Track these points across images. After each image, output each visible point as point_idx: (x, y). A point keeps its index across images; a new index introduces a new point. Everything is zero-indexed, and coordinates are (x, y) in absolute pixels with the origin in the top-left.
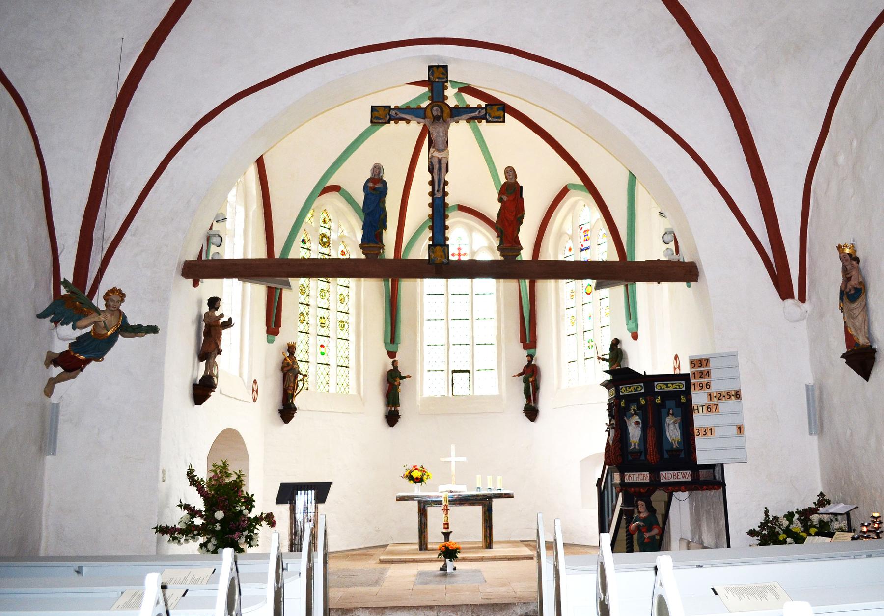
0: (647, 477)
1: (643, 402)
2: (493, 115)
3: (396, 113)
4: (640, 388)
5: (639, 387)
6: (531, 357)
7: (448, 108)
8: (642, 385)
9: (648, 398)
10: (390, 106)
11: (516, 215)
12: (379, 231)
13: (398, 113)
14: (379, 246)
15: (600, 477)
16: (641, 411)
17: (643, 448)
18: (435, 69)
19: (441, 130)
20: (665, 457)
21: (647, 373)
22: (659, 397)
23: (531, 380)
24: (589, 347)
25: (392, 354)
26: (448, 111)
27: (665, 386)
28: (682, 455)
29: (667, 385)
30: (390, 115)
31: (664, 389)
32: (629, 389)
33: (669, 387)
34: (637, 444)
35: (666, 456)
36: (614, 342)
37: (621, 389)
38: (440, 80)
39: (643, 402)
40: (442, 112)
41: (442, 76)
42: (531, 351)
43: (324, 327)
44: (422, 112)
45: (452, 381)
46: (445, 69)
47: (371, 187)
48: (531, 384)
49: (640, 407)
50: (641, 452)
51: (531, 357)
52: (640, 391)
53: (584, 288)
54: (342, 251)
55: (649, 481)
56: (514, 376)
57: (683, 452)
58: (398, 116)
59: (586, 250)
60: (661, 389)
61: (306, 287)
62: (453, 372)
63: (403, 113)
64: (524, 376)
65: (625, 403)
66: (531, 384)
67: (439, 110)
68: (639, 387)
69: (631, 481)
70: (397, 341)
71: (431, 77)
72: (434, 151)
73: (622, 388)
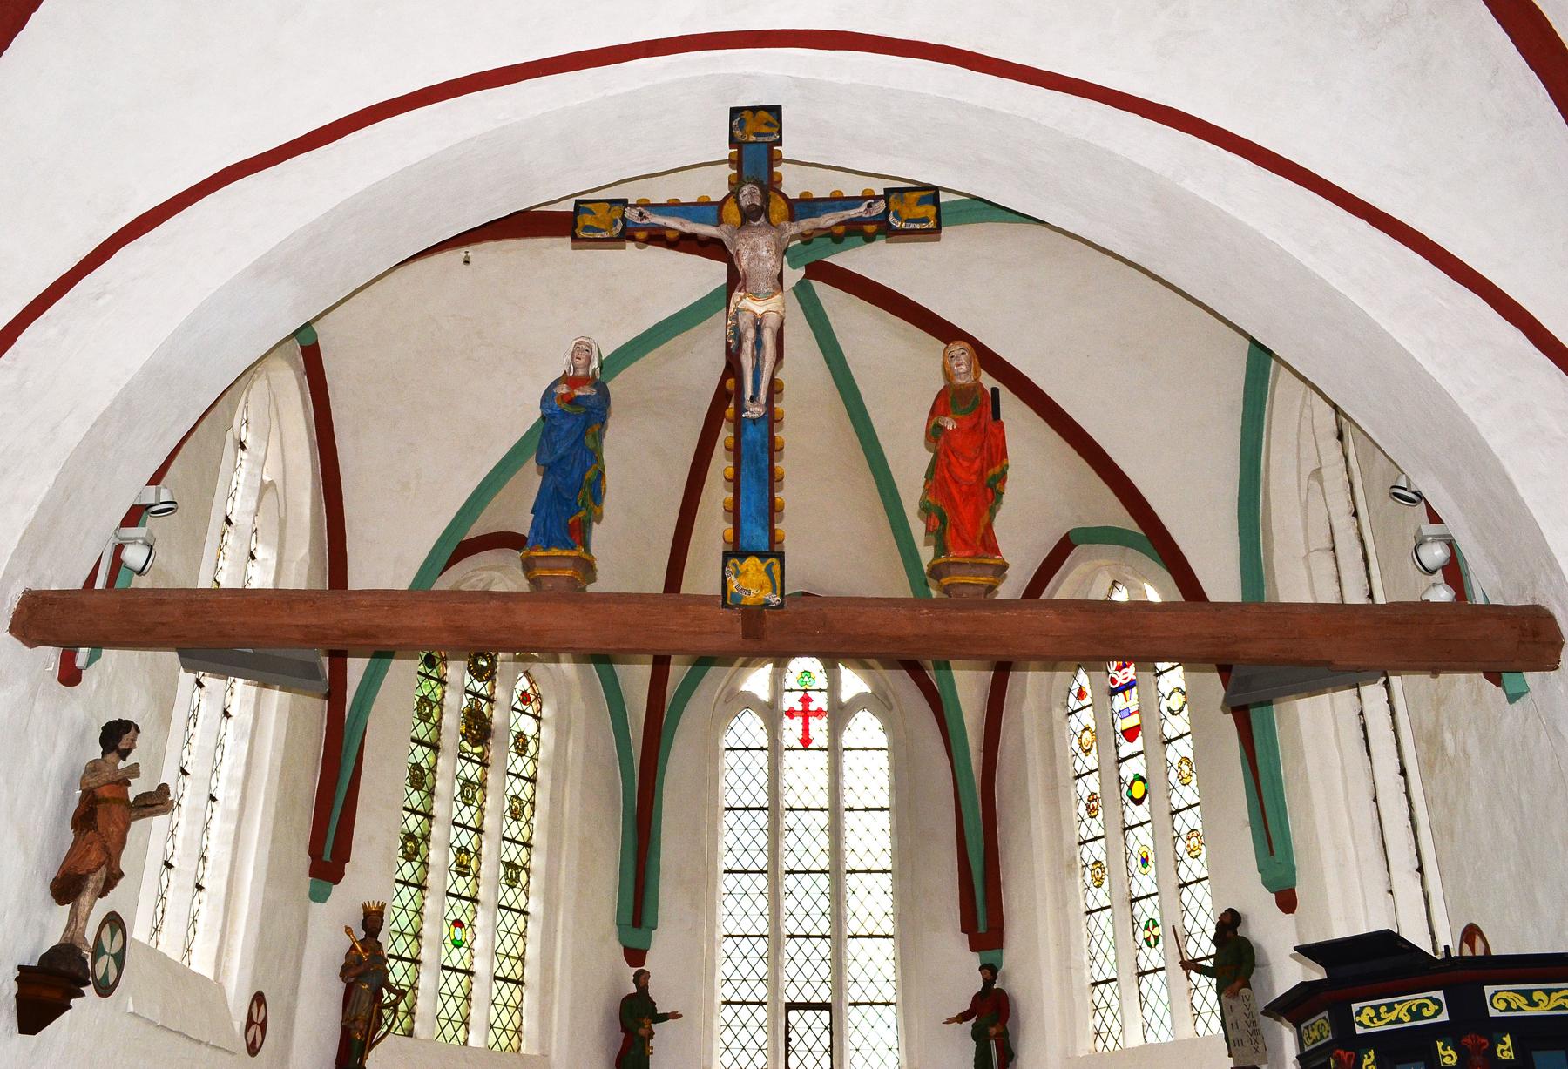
2: (906, 213)
3: (641, 214)
4: (1433, 1006)
6: (990, 971)
7: (782, 201)
8: (1439, 995)
9: (1467, 1040)
10: (627, 200)
11: (982, 471)
12: (581, 515)
13: (647, 213)
14: (574, 554)
18: (747, 115)
19: (761, 242)
22: (1507, 1039)
23: (993, 1031)
24: (1147, 940)
25: (635, 956)
26: (784, 207)
27: (1523, 1000)
29: (1527, 995)
30: (624, 219)
31: (1519, 1009)
32: (1388, 1012)
33: (1536, 1004)
36: (1228, 920)
37: (1359, 1013)
38: (761, 139)
40: (766, 199)
41: (765, 130)
42: (991, 956)
43: (468, 874)
44: (712, 212)
45: (787, 1033)
46: (775, 113)
47: (563, 396)
48: (993, 1043)
51: (990, 971)
52: (1434, 1016)
53: (1126, 788)
54: (524, 693)
56: (950, 1021)
58: (645, 222)
59: (1123, 691)
60: (1509, 1009)
61: (426, 772)
62: (792, 1006)
63: (660, 214)
64: (974, 1020)
66: (993, 1043)
67: (758, 193)
68: (1427, 1006)
70: (647, 919)
71: (738, 133)
72: (742, 298)
73: (1362, 1009)
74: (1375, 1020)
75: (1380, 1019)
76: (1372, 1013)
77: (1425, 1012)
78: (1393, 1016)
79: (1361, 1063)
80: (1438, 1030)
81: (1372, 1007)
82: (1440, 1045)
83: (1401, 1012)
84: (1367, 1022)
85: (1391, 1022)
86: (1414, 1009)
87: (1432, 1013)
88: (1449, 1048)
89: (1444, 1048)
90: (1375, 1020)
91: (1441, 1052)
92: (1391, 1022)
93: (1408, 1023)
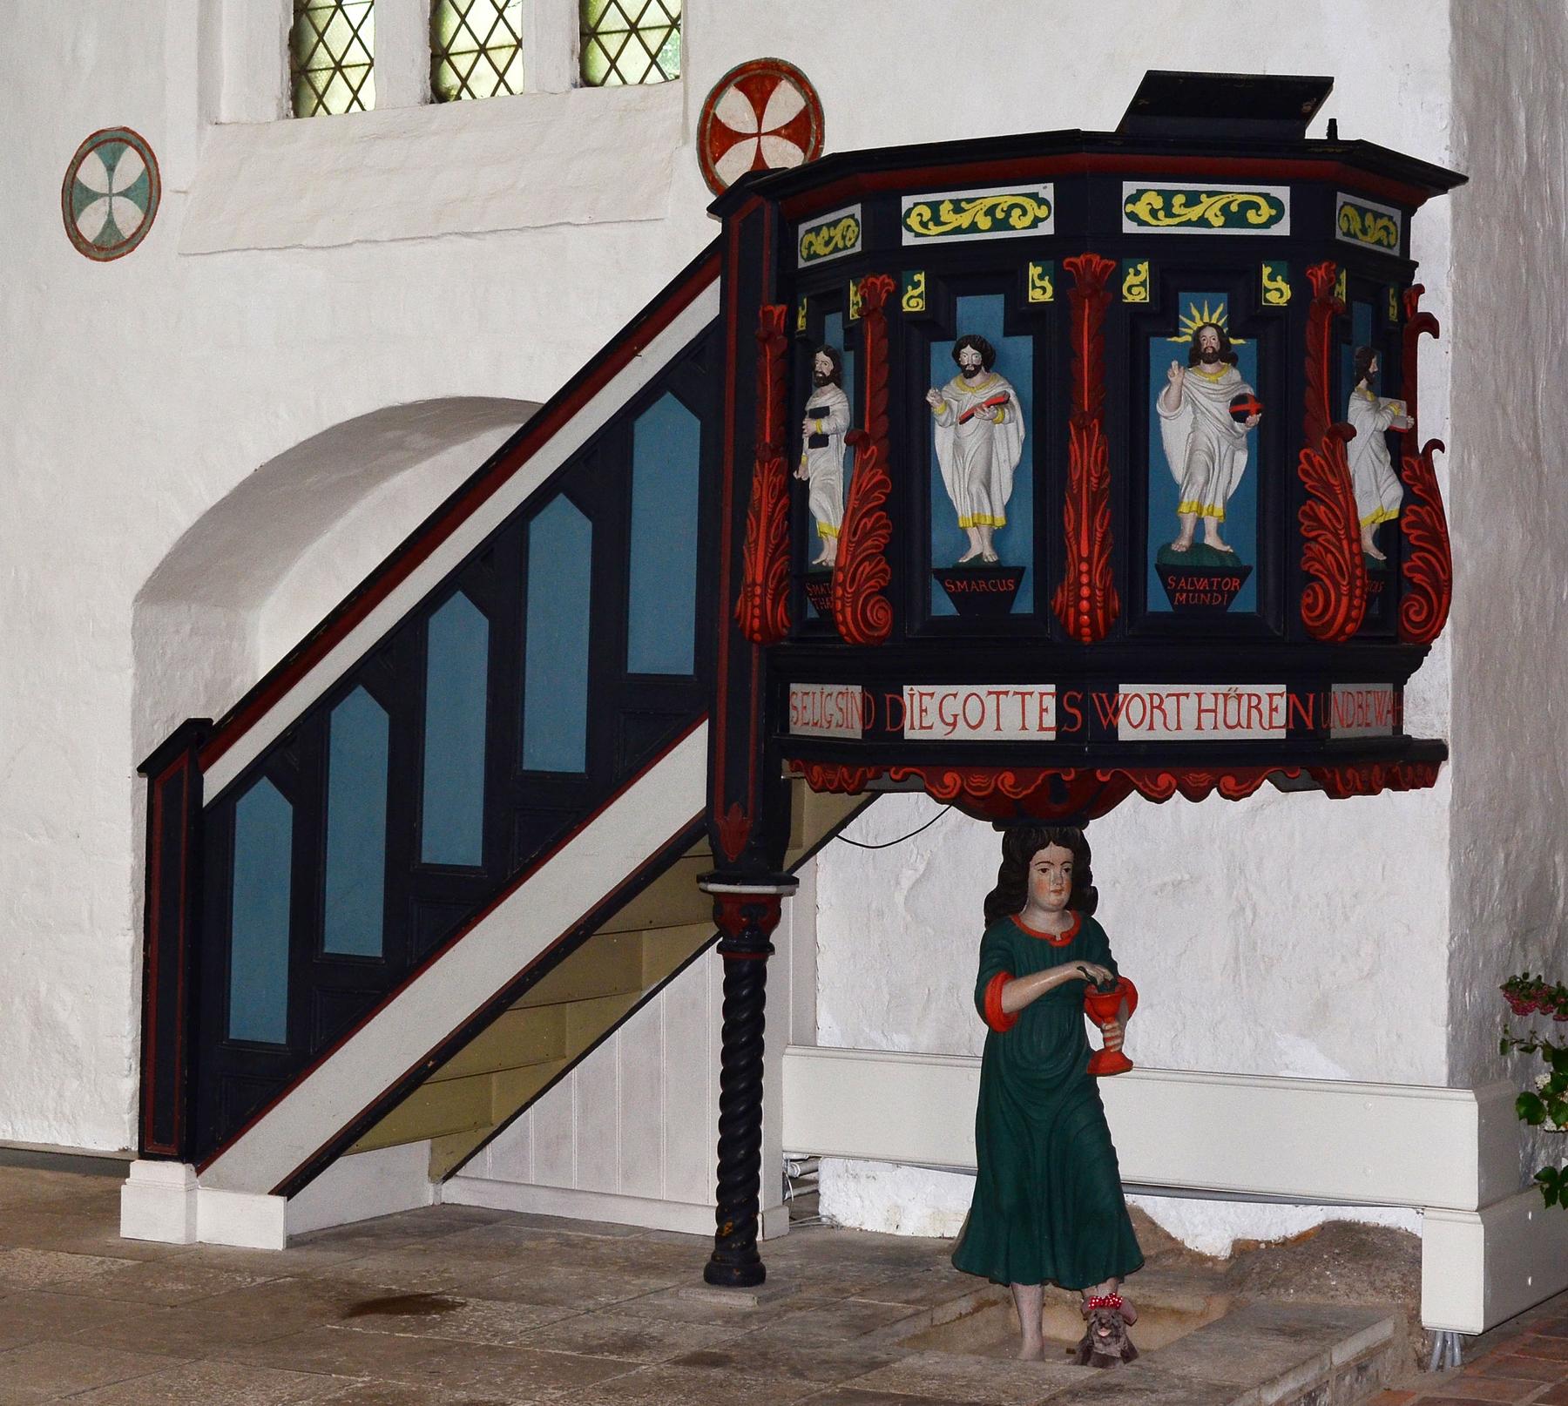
0: (1273, 710)
1: (1040, 291)
5: (1257, 207)
8: (1283, 193)
15: (216, 714)
16: (1253, 342)
17: (1022, 551)
20: (1152, 606)
21: (1342, 136)
28: (1024, 604)
32: (1187, 205)
34: (1211, 525)
35: (1158, 600)
37: (1134, 199)
39: (1277, 292)
49: (1021, 318)
50: (1242, 573)
52: (1266, 225)
57: (1252, 580)
65: (929, 296)
68: (1257, 207)
69: (1160, 734)
73: (1141, 193)
74: (1161, 214)
76: (1158, 203)
77: (1251, 216)
78: (1194, 213)
79: (1122, 281)
80: (1268, 248)
81: (1159, 192)
82: (1266, 271)
83: (1210, 209)
84: (1144, 214)
85: (1188, 223)
86: (1234, 208)
87: (1263, 219)
88: (1279, 278)
89: (1272, 278)
90: (1161, 214)
91: (1266, 282)
92: (1188, 223)
93: (1218, 228)
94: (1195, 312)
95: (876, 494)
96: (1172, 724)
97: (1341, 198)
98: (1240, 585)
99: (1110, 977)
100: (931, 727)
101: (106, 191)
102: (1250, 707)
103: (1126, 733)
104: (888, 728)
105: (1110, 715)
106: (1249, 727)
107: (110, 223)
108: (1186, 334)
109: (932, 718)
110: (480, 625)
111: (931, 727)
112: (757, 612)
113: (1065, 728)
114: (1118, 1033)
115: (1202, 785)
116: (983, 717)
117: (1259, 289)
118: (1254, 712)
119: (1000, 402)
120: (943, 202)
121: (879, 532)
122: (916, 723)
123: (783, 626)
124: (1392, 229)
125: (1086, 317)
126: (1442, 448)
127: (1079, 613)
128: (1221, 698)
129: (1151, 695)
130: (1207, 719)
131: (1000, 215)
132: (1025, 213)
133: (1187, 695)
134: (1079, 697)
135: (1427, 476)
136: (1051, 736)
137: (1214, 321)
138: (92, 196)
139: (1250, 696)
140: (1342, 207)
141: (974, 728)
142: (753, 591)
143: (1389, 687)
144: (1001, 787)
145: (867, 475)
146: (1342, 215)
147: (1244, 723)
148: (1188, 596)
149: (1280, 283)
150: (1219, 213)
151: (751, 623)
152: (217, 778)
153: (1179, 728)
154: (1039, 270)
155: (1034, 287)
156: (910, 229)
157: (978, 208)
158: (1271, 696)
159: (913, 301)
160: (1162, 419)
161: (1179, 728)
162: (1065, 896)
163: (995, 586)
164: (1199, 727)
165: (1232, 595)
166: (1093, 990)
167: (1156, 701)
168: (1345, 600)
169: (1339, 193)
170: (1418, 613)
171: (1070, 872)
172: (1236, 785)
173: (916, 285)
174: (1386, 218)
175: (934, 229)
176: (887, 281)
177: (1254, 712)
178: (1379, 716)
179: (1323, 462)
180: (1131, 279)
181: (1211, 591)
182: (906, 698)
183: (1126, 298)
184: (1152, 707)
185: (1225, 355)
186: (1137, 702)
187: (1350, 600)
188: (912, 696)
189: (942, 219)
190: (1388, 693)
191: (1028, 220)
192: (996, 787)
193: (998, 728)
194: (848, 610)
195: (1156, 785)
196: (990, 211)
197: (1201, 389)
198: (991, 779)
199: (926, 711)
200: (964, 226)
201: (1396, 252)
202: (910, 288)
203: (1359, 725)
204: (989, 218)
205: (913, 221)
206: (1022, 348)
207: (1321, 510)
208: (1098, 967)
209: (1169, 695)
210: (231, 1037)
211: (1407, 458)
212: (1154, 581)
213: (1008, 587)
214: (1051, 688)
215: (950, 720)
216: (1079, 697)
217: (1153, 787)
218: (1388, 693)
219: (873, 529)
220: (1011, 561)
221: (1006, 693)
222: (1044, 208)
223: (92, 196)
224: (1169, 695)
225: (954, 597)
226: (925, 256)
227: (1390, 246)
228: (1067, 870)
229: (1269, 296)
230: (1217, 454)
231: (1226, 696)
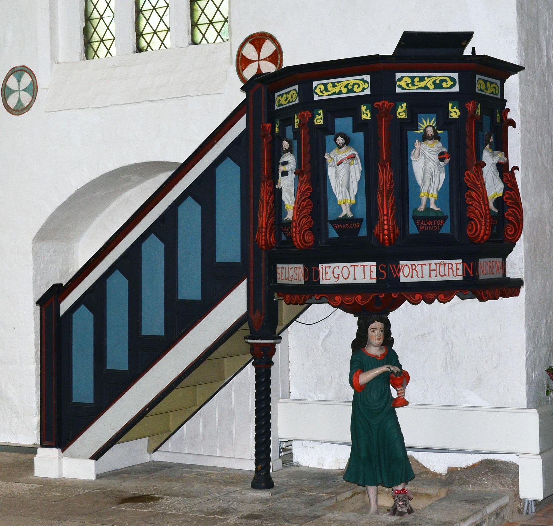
0: (457, 269)
1: (366, 115)
5: (446, 81)
8: (456, 76)
15: (64, 282)
17: (362, 213)
21: (478, 53)
28: (363, 232)
32: (420, 81)
34: (432, 200)
35: (413, 229)
37: (400, 79)
39: (455, 113)
49: (359, 125)
50: (444, 218)
55: (461, 278)
57: (448, 221)
65: (325, 118)
68: (446, 81)
69: (415, 279)
73: (402, 78)
74: (410, 85)
75: (413, 85)
76: (409, 81)
77: (444, 85)
78: (423, 84)
81: (410, 77)
83: (429, 82)
84: (404, 85)
85: (421, 88)
86: (438, 82)
88: (455, 107)
89: (452, 108)
90: (410, 85)
91: (450, 109)
92: (421, 88)
94: (424, 122)
95: (307, 193)
96: (420, 275)
97: (478, 77)
98: (444, 223)
99: (399, 370)
100: (329, 279)
101: (17, 89)
102: (449, 268)
103: (403, 279)
104: (314, 280)
105: (397, 273)
106: (449, 275)
107: (19, 101)
108: (421, 129)
109: (330, 276)
110: (161, 246)
111: (329, 279)
112: (264, 238)
113: (380, 278)
114: (403, 391)
115: (432, 298)
116: (349, 275)
117: (447, 112)
118: (450, 270)
119: (352, 157)
120: (328, 83)
121: (308, 207)
122: (324, 278)
123: (274, 243)
124: (497, 87)
125: (383, 124)
126: (518, 169)
127: (384, 235)
128: (438, 265)
129: (412, 265)
130: (433, 273)
131: (350, 87)
132: (359, 86)
133: (425, 264)
134: (385, 266)
135: (512, 180)
136: (375, 281)
137: (431, 124)
138: (13, 91)
139: (449, 264)
140: (478, 80)
141: (346, 279)
142: (262, 230)
143: (500, 259)
144: (356, 300)
145: (303, 186)
146: (478, 84)
147: (447, 274)
148: (424, 227)
149: (456, 109)
150: (432, 84)
151: (262, 242)
152: (65, 305)
153: (422, 277)
154: (365, 107)
155: (364, 114)
156: (316, 94)
157: (342, 85)
158: (457, 264)
159: (319, 120)
160: (413, 162)
161: (422, 277)
162: (381, 341)
163: (352, 226)
164: (430, 276)
165: (441, 226)
166: (393, 375)
167: (414, 267)
168: (483, 227)
169: (476, 75)
170: (511, 231)
171: (383, 332)
172: (444, 297)
173: (319, 115)
174: (494, 84)
175: (325, 93)
176: (308, 113)
177: (450, 270)
178: (497, 271)
179: (474, 176)
180: (400, 110)
181: (433, 225)
182: (320, 269)
183: (398, 117)
184: (412, 269)
185: (436, 137)
186: (406, 267)
187: (485, 228)
188: (322, 268)
189: (329, 90)
190: (500, 262)
191: (360, 89)
192: (355, 301)
193: (355, 279)
194: (298, 237)
195: (415, 299)
196: (346, 86)
197: (428, 150)
198: (353, 298)
199: (328, 273)
200: (336, 92)
201: (499, 96)
202: (317, 116)
203: (490, 274)
204: (346, 89)
205: (318, 91)
206: (360, 137)
207: (473, 194)
208: (395, 367)
209: (418, 265)
210: (73, 401)
211: (505, 173)
212: (411, 221)
213: (357, 226)
214: (374, 263)
215: (337, 276)
216: (385, 266)
217: (413, 299)
218: (500, 262)
219: (306, 206)
220: (358, 216)
221: (357, 266)
222: (366, 84)
223: (13, 91)
224: (418, 265)
225: (337, 231)
226: (322, 104)
227: (496, 94)
228: (382, 331)
229: (452, 114)
230: (434, 174)
231: (440, 264)
